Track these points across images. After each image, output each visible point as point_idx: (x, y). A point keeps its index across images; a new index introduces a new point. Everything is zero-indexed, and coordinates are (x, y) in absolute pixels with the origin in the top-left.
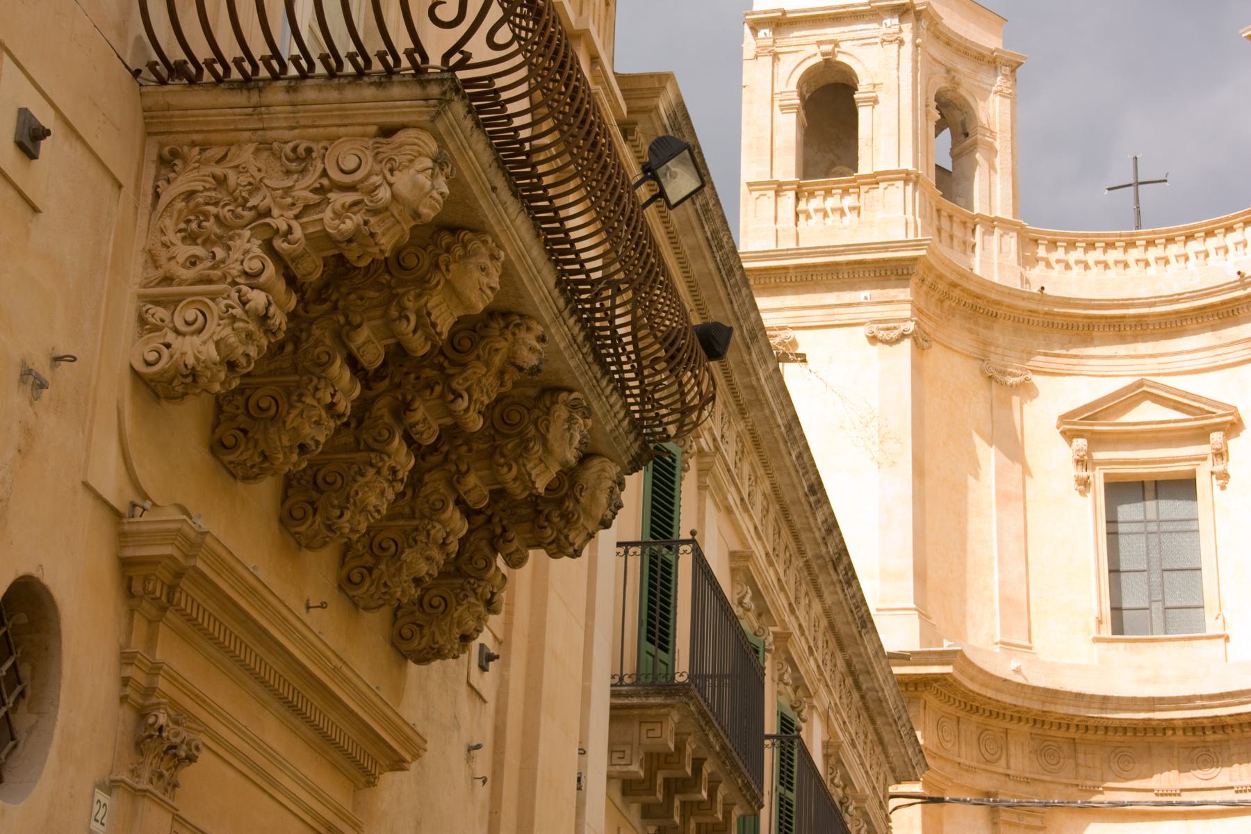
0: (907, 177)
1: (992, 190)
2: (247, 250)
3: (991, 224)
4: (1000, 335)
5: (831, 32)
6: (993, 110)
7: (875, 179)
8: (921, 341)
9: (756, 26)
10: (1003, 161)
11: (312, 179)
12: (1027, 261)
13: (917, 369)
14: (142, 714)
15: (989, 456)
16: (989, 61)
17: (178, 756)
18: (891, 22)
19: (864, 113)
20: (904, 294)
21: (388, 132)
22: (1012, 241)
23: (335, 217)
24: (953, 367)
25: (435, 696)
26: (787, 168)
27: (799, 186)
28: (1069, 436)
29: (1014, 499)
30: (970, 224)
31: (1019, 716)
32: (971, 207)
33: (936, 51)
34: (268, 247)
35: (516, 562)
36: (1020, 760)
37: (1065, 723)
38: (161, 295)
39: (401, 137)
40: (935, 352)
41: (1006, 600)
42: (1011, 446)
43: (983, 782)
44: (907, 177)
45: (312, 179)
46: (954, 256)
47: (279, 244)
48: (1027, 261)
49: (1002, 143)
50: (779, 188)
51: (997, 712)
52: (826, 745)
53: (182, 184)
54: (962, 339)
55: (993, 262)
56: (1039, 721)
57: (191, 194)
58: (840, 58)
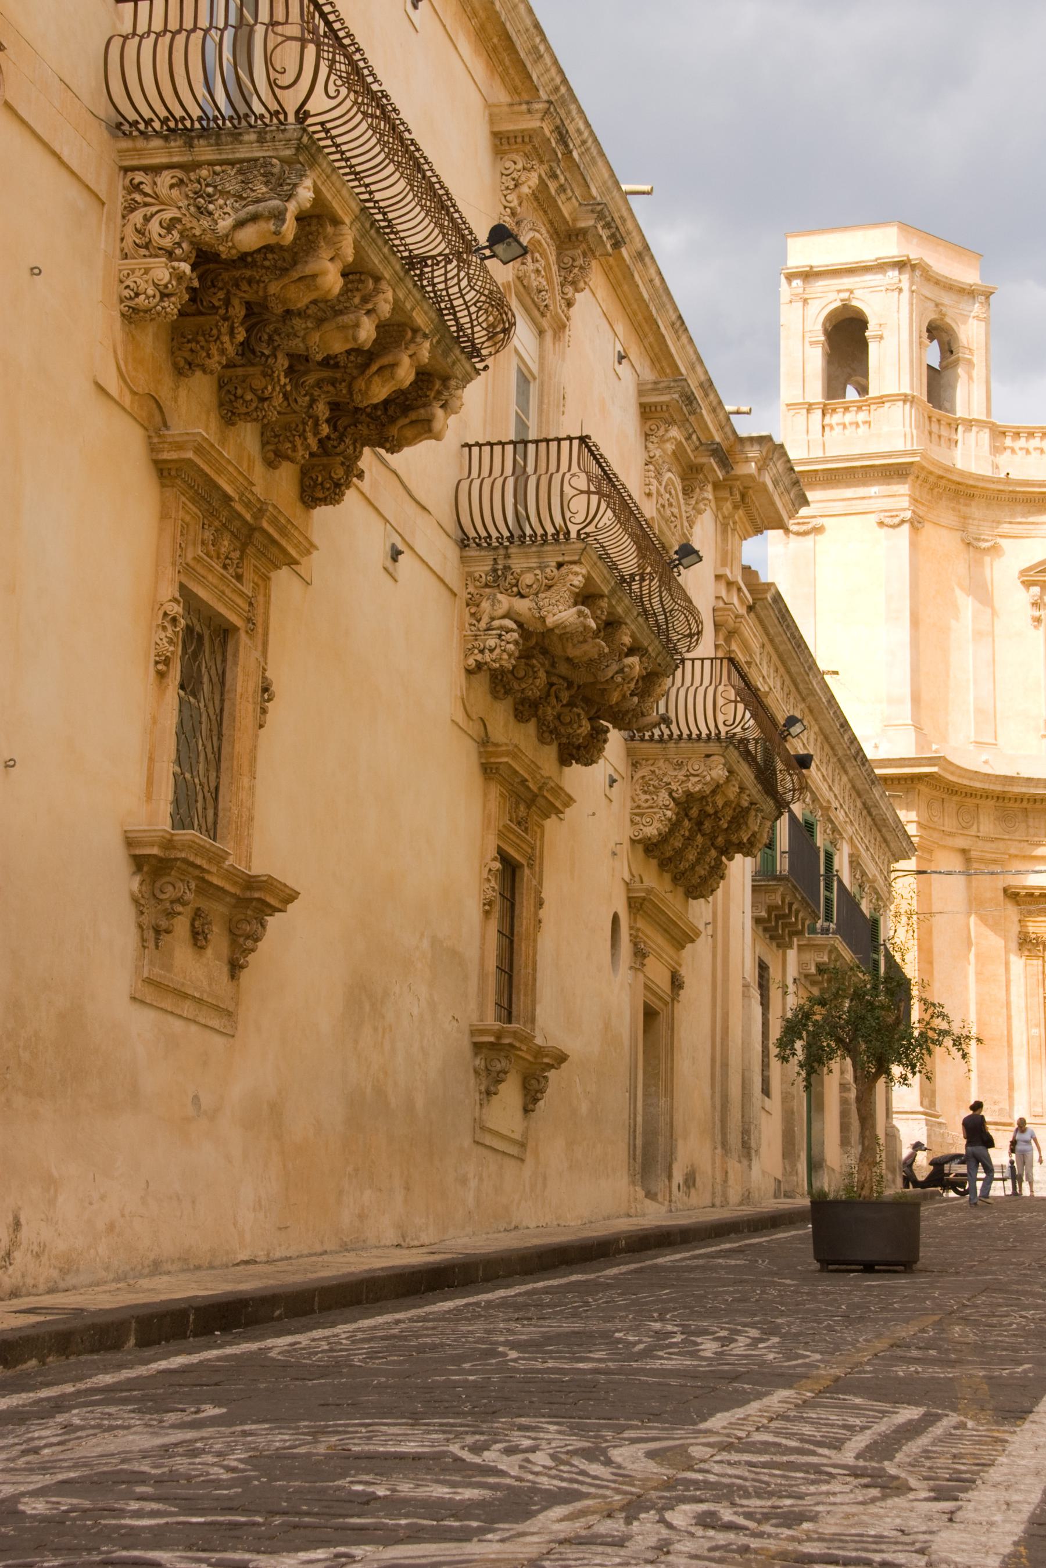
0: (905, 399)
1: (968, 396)
2: (663, 796)
3: (969, 423)
4: (976, 510)
5: (847, 282)
6: (971, 331)
7: (881, 400)
8: (916, 524)
9: (790, 277)
10: (979, 371)
11: (684, 772)
12: (997, 450)
13: (913, 545)
14: (635, 944)
15: (967, 604)
16: (969, 293)
17: (644, 956)
18: (893, 274)
19: (872, 347)
20: (903, 489)
21: (708, 756)
22: (985, 435)
23: (694, 786)
24: (942, 539)
25: (700, 911)
26: (816, 391)
27: (825, 405)
28: (1028, 584)
29: (984, 635)
30: (954, 425)
31: (986, 795)
32: (953, 411)
33: (928, 291)
34: (670, 795)
35: (731, 859)
36: (987, 826)
37: (1020, 798)
38: (637, 813)
39: (712, 758)
40: (928, 529)
41: (978, 711)
42: (982, 593)
43: (961, 842)
44: (905, 399)
45: (684, 772)
46: (939, 454)
47: (675, 795)
48: (997, 450)
49: (978, 359)
50: (810, 408)
51: (970, 793)
52: (851, 856)
53: (640, 774)
54: (948, 517)
55: (970, 456)
56: (1001, 797)
57: (643, 777)
58: (854, 303)
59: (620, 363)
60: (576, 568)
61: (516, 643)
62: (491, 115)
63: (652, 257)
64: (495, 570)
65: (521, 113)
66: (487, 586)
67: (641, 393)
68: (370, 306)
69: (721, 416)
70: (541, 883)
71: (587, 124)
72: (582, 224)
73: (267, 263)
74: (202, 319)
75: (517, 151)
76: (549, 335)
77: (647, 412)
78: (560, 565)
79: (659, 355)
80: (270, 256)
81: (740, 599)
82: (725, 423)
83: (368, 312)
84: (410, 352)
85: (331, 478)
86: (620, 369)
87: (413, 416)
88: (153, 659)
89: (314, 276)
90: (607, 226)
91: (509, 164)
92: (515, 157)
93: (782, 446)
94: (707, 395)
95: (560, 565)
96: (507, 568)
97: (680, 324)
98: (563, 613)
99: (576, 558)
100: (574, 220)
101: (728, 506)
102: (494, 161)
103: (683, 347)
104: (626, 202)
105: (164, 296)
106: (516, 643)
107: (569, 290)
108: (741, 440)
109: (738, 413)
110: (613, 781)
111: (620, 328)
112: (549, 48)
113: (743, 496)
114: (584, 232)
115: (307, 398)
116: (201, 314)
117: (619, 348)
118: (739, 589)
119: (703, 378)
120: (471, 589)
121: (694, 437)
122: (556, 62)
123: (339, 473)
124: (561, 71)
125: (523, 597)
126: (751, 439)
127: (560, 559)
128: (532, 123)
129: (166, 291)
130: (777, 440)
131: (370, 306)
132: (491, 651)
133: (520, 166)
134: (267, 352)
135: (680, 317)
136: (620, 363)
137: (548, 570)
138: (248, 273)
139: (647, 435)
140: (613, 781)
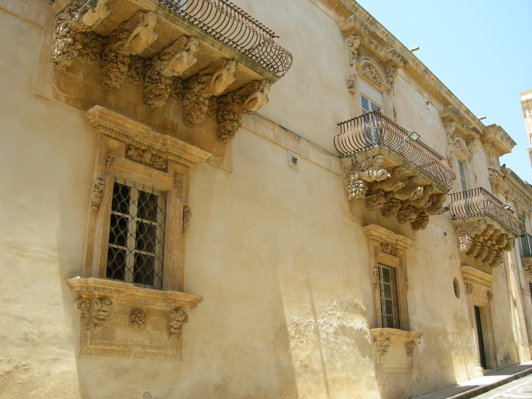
53: (458, 230)
59: (427, 104)
60: (380, 156)
61: (363, 188)
62: (339, 26)
63: (430, 71)
64: (353, 164)
65: (348, 22)
66: (351, 170)
67: (440, 114)
68: (187, 48)
69: (477, 120)
70: (406, 273)
71: (385, 29)
72: (389, 58)
73: (124, 36)
74: (108, 66)
75: (351, 34)
76: (385, 94)
77: (444, 120)
78: (374, 157)
79: (446, 103)
80: (125, 33)
81: (498, 174)
82: (479, 122)
83: (188, 50)
85: (227, 129)
86: (428, 107)
87: (250, 98)
88: (91, 204)
89: (138, 34)
90: (399, 56)
91: (349, 39)
92: (350, 36)
93: (500, 126)
94: (469, 115)
95: (374, 157)
96: (356, 162)
97: (449, 92)
98: (376, 174)
99: (378, 153)
100: (386, 58)
101: (488, 148)
102: (344, 40)
103: (454, 100)
104: (412, 54)
105: (64, 53)
106: (363, 188)
107: (390, 79)
108: (487, 127)
109: (482, 119)
110: (445, 234)
111: (426, 95)
112: (359, 5)
113: (492, 144)
114: (391, 60)
115: (196, 97)
116: (108, 64)
117: (426, 100)
118: (498, 172)
119: (465, 109)
120: (346, 173)
121: (465, 126)
122: (364, 10)
123: (229, 127)
124: (367, 13)
125: (364, 171)
126: (490, 126)
127: (373, 154)
128: (351, 24)
129: (65, 51)
130: (498, 125)
131: (187, 48)
132: (355, 192)
133: (352, 38)
134: (157, 78)
135: (449, 90)
136: (427, 104)
137: (370, 159)
138: (120, 42)
139: (445, 126)
140: (445, 234)
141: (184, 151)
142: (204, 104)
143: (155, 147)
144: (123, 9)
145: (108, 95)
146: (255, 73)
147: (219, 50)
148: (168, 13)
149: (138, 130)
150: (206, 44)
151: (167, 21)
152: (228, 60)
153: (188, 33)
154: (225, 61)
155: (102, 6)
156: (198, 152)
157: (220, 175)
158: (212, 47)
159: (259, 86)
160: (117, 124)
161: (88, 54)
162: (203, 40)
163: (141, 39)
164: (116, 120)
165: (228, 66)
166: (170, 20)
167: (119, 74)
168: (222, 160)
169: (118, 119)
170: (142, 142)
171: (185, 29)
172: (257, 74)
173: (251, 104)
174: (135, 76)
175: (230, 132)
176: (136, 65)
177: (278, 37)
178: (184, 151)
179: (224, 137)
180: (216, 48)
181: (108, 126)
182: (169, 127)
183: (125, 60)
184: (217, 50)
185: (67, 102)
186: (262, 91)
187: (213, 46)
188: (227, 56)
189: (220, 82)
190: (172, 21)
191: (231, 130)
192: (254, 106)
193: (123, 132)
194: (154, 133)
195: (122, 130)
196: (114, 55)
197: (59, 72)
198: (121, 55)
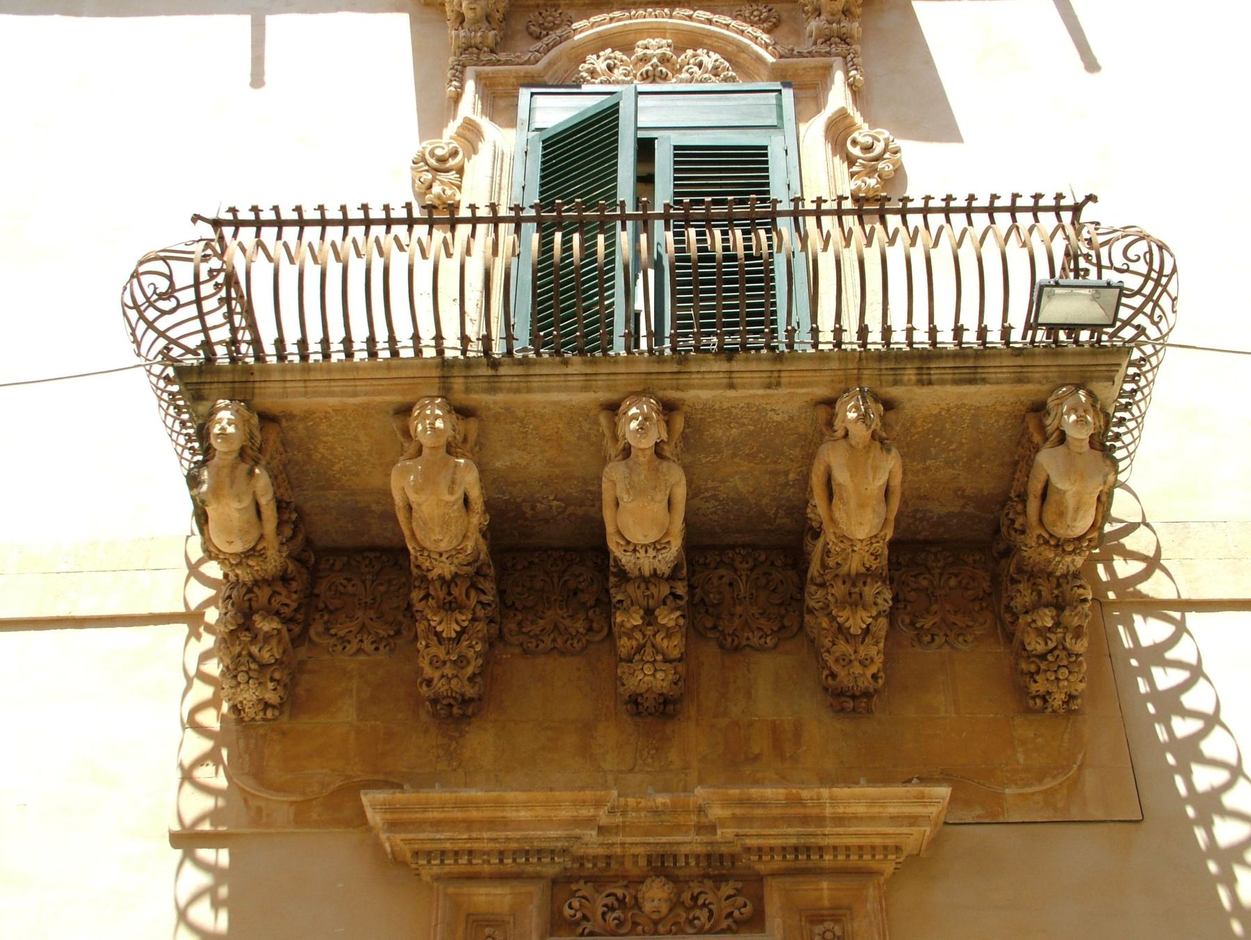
84: (840, 433)
131: (621, 445)
141: (805, 820)
142: (855, 602)
143: (685, 849)
144: (356, 439)
145: (462, 736)
146: (986, 388)
147: (769, 386)
148: (490, 372)
149: (565, 813)
150: (705, 394)
151: (500, 397)
152: (830, 403)
153: (604, 396)
154: (822, 413)
155: (226, 471)
156: (873, 802)
157: (1078, 852)
158: (731, 393)
159: (1042, 428)
160: (469, 824)
161: (363, 628)
162: (678, 389)
163: (419, 505)
164: (459, 815)
165: (838, 424)
166: (510, 390)
167: (441, 652)
168: (1074, 785)
169: (463, 805)
170: (619, 850)
171: (586, 389)
172: (1006, 387)
173: (1049, 517)
174: (567, 622)
175: (1043, 657)
176: (572, 584)
177: (1091, 198)
178: (805, 820)
179: (1039, 686)
180: (752, 386)
181: (448, 846)
182: (757, 750)
183: (455, 591)
184: (761, 392)
185: (300, 820)
186: (1062, 438)
187: (731, 386)
188: (822, 392)
189: (841, 498)
190: (518, 391)
191: (1040, 648)
192: (1061, 514)
193: (514, 845)
194: (643, 803)
195: (508, 839)
196: (422, 594)
197: (262, 731)
198: (438, 584)
